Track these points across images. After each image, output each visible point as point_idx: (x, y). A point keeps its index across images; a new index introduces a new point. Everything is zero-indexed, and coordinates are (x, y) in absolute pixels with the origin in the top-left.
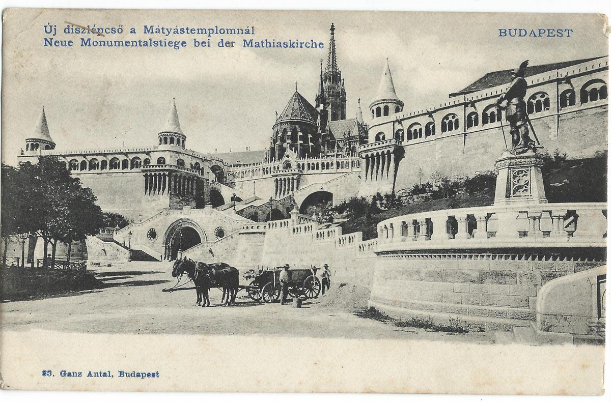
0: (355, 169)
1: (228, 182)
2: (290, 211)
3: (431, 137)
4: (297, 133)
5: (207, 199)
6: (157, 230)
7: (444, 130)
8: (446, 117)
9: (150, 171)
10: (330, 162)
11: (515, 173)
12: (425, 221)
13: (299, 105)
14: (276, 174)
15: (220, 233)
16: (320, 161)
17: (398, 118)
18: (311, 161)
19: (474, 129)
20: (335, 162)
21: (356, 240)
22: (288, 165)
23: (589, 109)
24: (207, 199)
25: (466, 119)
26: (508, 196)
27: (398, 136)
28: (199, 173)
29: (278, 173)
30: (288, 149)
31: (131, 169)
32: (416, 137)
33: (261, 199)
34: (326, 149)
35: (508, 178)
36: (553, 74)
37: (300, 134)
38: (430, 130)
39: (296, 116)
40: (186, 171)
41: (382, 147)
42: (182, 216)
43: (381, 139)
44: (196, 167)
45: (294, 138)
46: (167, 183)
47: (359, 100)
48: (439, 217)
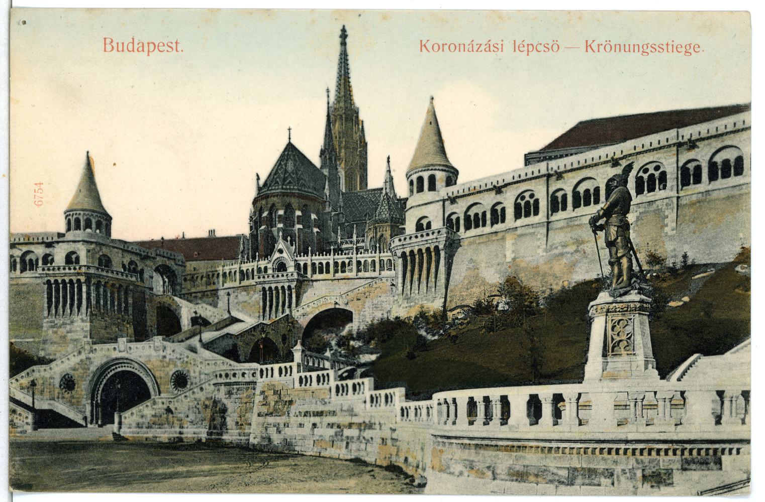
0: (386, 273)
1: (184, 292)
2: (292, 348)
3: (499, 227)
4: (293, 213)
5: (151, 319)
6: (76, 375)
7: (518, 216)
8: (521, 196)
9: (54, 275)
10: (347, 261)
11: (615, 323)
12: (499, 399)
13: (295, 165)
14: (262, 279)
15: (181, 380)
16: (330, 259)
17: (450, 194)
18: (318, 259)
19: (560, 215)
20: (354, 261)
21: (396, 399)
22: (282, 267)
23: (719, 189)
24: (151, 319)
25: (550, 199)
26: (604, 355)
27: (450, 223)
28: (137, 279)
29: (266, 279)
30: (281, 240)
31: (21, 272)
32: (477, 226)
33: (243, 321)
34: (339, 237)
35: (606, 330)
36: (671, 135)
37: (298, 213)
38: (498, 216)
39: (290, 182)
40: (115, 276)
41: (427, 240)
42: (115, 355)
43: (425, 227)
44: (132, 268)
45: (288, 220)
46: (84, 296)
47: (389, 158)
48: (519, 396)
